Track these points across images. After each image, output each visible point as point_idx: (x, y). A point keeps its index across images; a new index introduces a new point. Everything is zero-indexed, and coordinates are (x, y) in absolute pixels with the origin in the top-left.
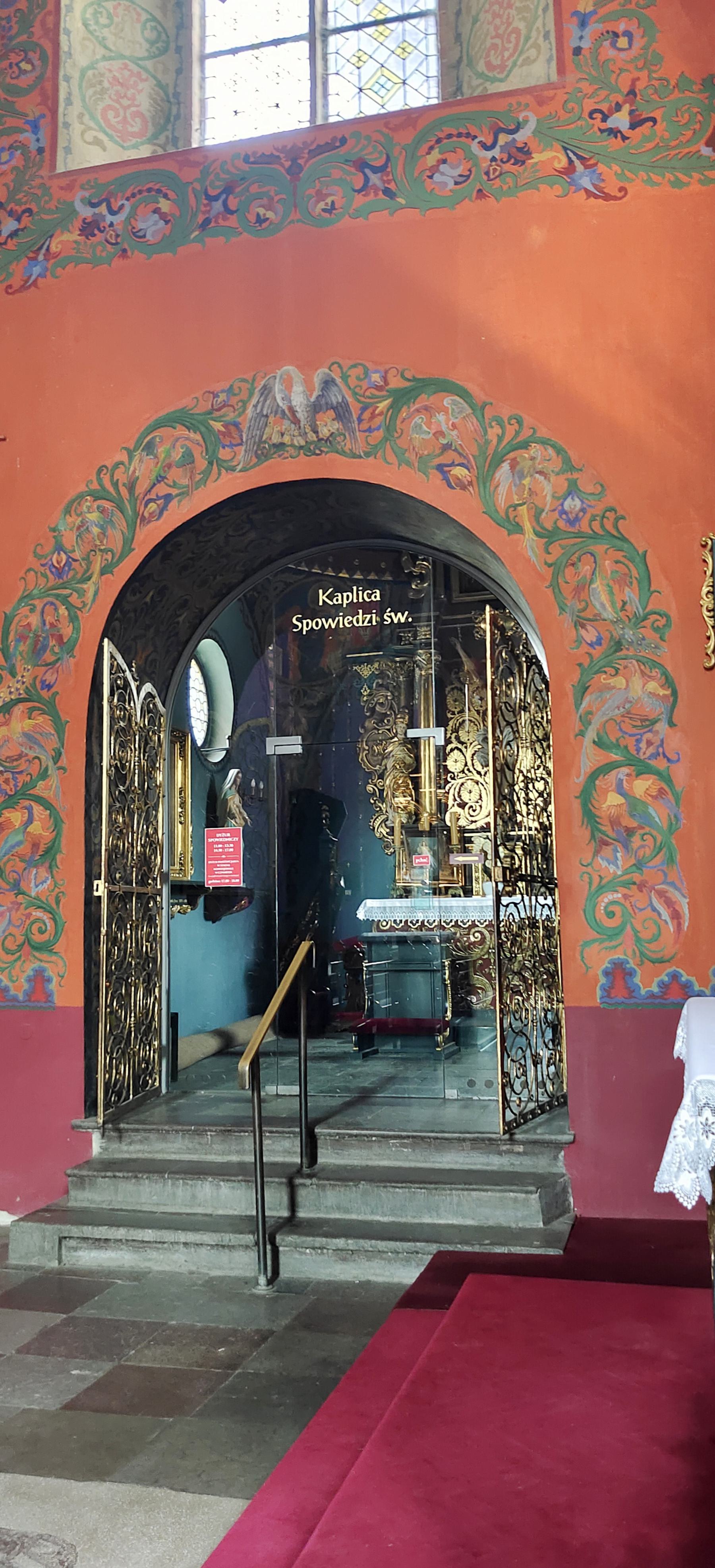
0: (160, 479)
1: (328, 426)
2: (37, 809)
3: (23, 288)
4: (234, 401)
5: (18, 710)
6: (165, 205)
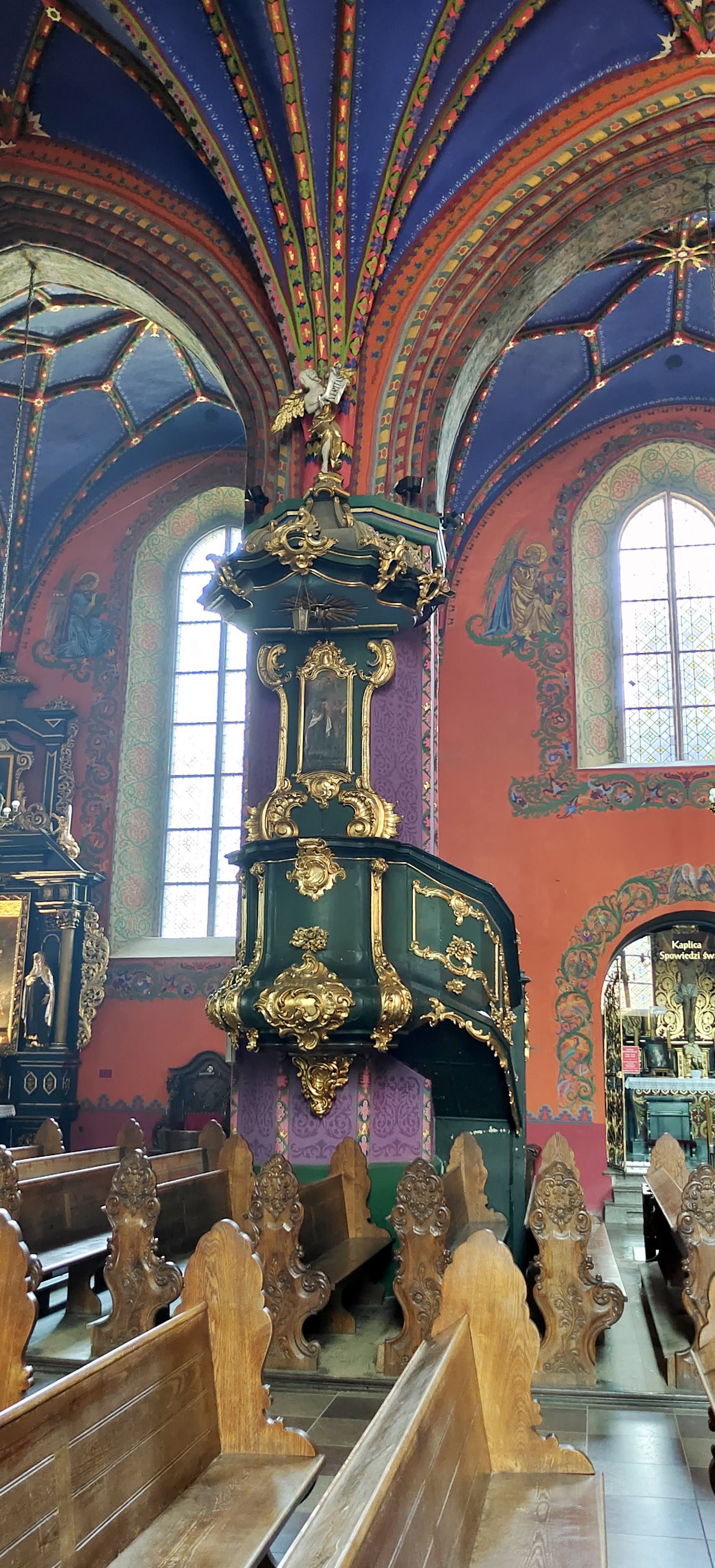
0: (632, 904)
1: (705, 890)
2: (581, 1039)
3: (565, 817)
4: (664, 875)
5: (570, 997)
6: (629, 790)
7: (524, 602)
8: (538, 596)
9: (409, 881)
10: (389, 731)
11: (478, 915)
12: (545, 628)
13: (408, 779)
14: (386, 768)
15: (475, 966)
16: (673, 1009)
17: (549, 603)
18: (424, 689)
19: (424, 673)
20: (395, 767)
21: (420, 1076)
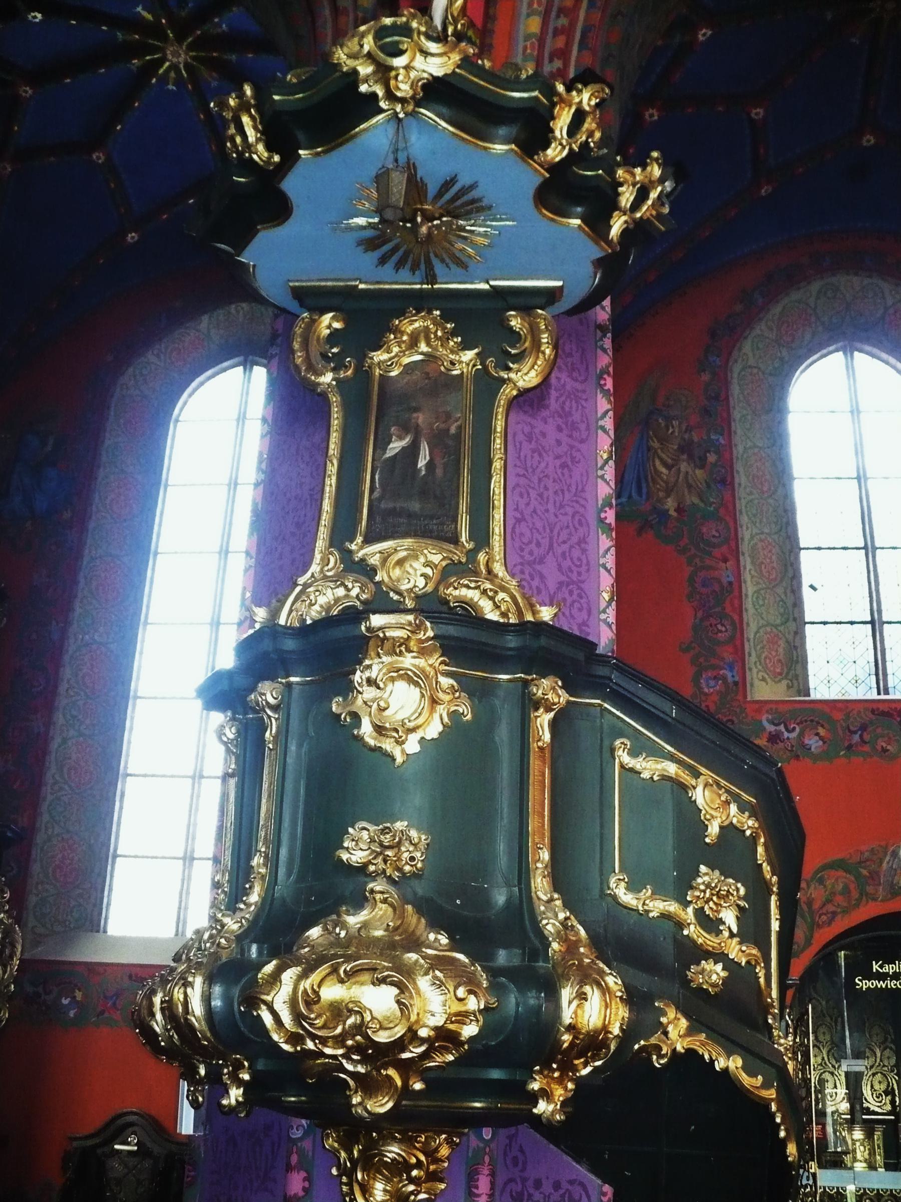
0: (828, 901)
4: (875, 858)
6: (821, 731)
7: (665, 464)
8: (685, 457)
9: (606, 743)
10: (540, 480)
11: (749, 824)
12: (696, 500)
13: (574, 577)
14: (533, 546)
15: (744, 936)
16: (832, 1069)
17: (702, 467)
18: (601, 423)
19: (600, 396)
20: (551, 547)
21: (592, 1177)
